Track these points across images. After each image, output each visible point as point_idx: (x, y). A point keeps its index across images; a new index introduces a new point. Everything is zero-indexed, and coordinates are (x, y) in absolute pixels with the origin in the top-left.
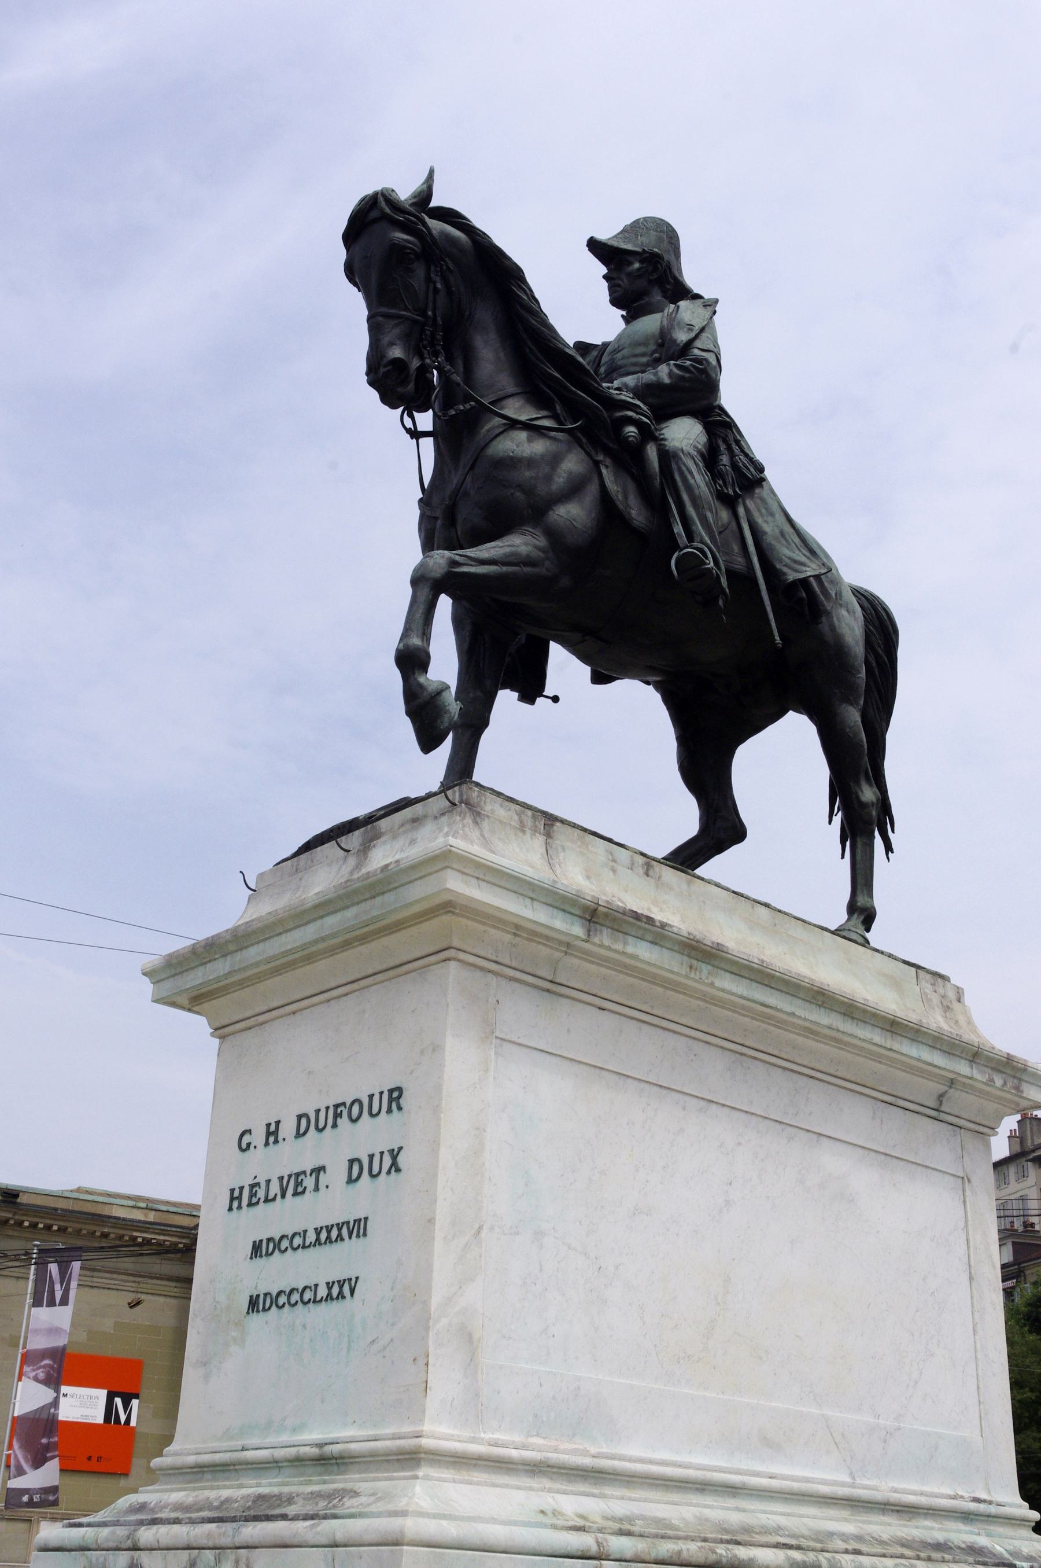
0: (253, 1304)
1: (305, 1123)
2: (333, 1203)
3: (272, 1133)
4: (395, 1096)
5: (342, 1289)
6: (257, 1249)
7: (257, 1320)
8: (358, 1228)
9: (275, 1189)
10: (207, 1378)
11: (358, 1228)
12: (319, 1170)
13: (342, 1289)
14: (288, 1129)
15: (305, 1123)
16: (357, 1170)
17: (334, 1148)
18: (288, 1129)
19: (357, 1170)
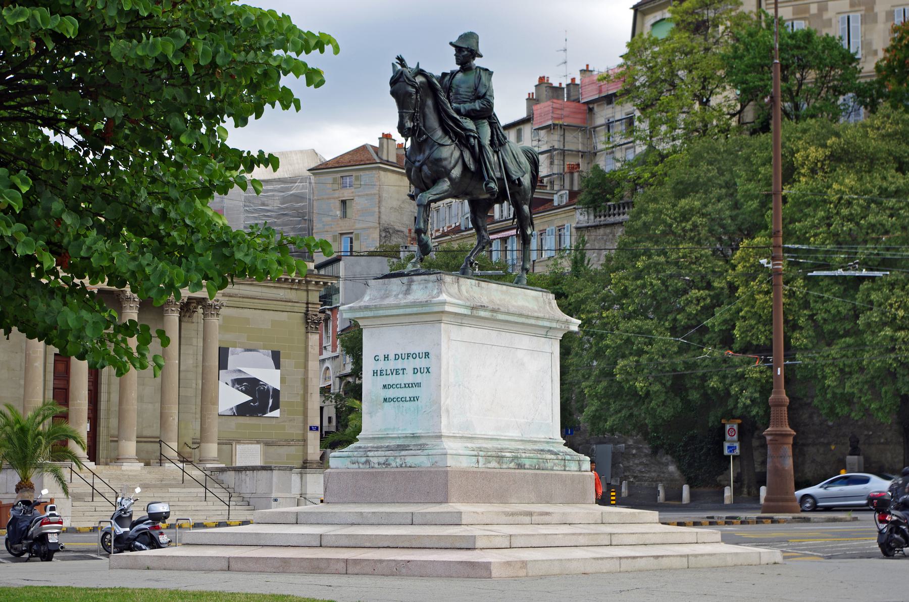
0: (385, 400)
1: (397, 357)
2: (409, 378)
3: (386, 358)
4: (427, 355)
5: (414, 399)
6: (385, 386)
7: (386, 404)
8: (418, 385)
9: (389, 372)
10: (371, 417)
11: (418, 385)
12: (403, 369)
13: (414, 399)
14: (392, 357)
15: (397, 357)
16: (415, 371)
17: (409, 365)
18: (392, 357)
19: (415, 371)
